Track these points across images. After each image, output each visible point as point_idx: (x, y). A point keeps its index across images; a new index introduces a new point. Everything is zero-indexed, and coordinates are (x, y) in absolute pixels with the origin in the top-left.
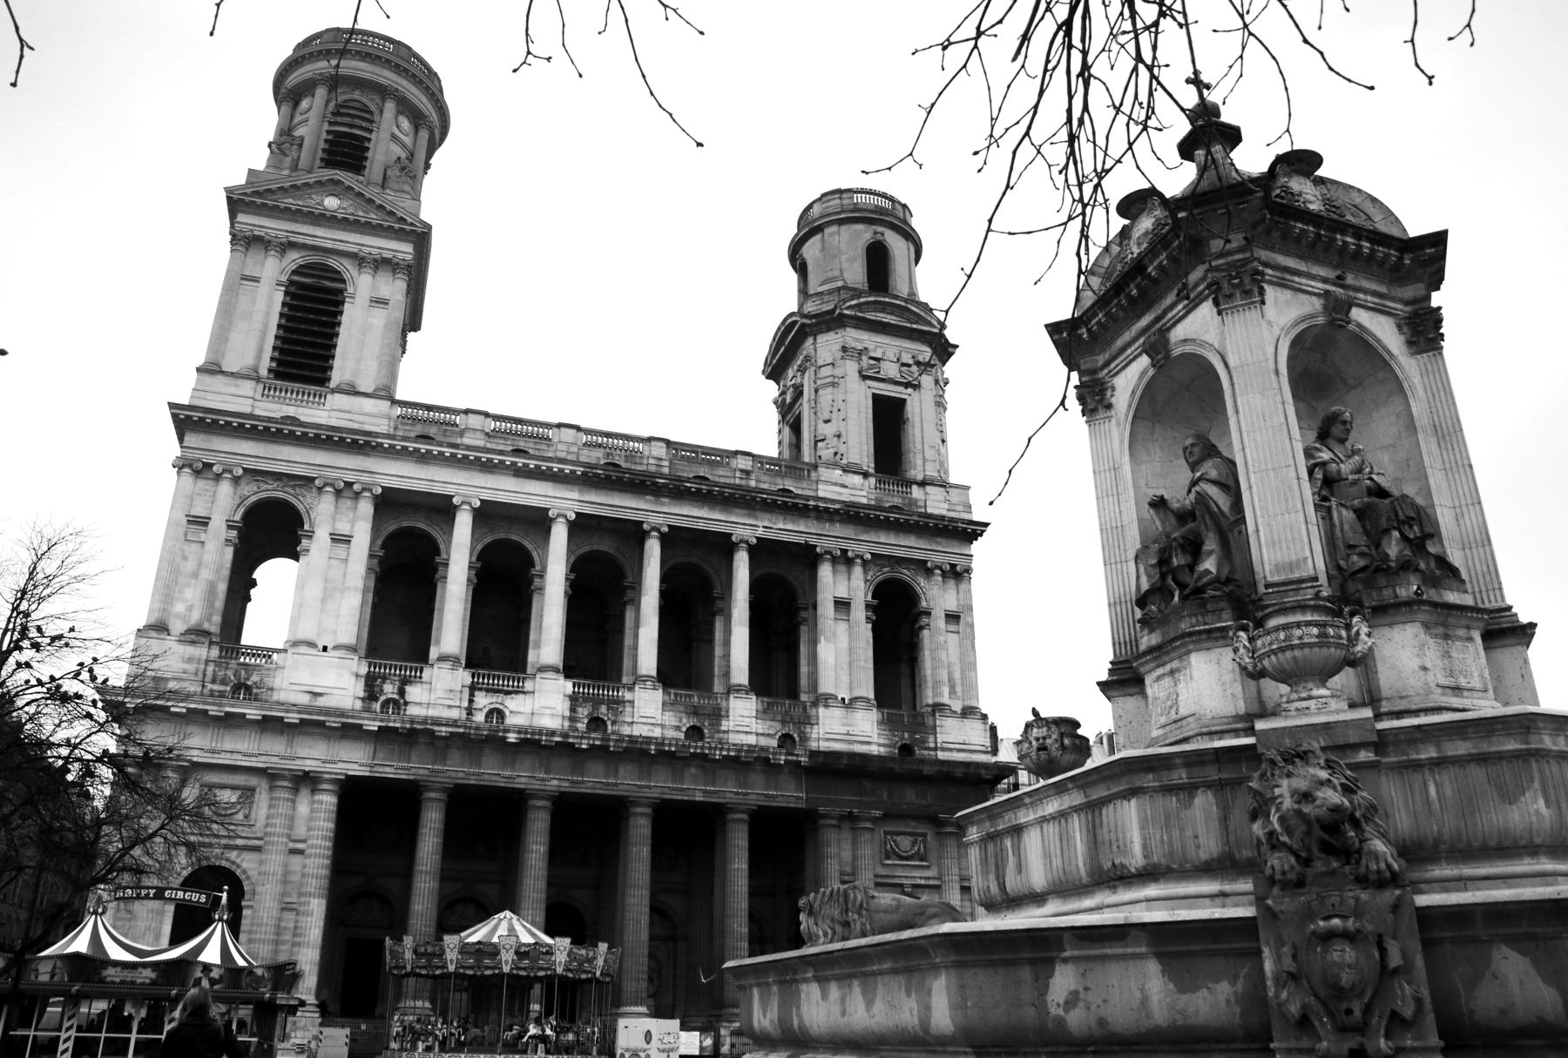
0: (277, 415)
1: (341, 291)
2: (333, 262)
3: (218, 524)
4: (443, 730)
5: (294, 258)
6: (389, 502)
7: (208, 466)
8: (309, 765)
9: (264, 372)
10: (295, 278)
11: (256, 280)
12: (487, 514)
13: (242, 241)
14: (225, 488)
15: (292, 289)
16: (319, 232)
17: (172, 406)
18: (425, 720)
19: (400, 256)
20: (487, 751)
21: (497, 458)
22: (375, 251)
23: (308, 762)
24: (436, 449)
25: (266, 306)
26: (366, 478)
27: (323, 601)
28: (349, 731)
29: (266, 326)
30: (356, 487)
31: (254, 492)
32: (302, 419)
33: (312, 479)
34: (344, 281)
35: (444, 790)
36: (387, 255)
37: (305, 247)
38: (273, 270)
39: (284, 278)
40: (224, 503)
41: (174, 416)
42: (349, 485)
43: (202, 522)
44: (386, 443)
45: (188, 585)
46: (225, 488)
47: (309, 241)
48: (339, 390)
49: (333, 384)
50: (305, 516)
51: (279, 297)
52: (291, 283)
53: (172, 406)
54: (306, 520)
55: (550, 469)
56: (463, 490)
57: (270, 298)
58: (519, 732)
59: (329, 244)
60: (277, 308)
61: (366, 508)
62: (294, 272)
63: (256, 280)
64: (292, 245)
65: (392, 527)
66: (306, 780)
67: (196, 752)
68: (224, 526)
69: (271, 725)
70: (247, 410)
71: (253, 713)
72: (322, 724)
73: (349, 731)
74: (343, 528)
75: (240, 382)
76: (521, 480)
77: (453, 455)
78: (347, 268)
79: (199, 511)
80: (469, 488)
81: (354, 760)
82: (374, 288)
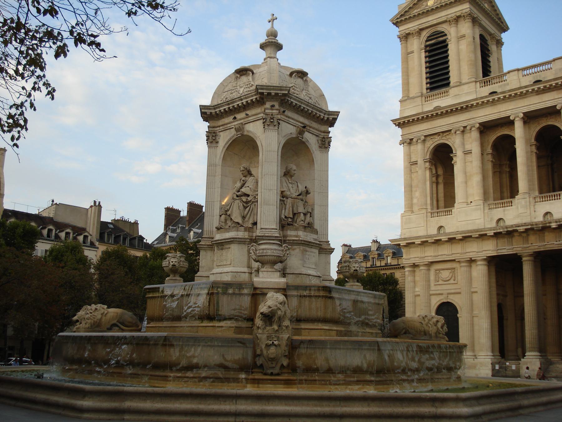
0: (431, 108)
1: (445, 41)
2: (440, 28)
3: (420, 161)
4: (521, 229)
5: (425, 34)
6: (485, 128)
7: (411, 140)
8: (472, 255)
9: (425, 91)
10: (428, 43)
11: (412, 52)
12: (529, 118)
13: (405, 37)
14: (419, 147)
15: (428, 48)
16: (430, 18)
17: (392, 121)
18: (512, 226)
19: (464, 11)
20: (546, 234)
21: (524, 90)
22: (453, 15)
23: (471, 254)
24: (496, 97)
25: (419, 61)
26: (472, 122)
27: (466, 183)
28: (483, 237)
29: (421, 71)
30: (468, 128)
31: (431, 144)
32: (442, 105)
33: (450, 130)
34: (446, 35)
35: (530, 255)
36: (458, 14)
37: (427, 28)
38: (417, 45)
39: (423, 46)
40: (421, 152)
41: (395, 124)
42: (465, 127)
43: (415, 163)
44: (474, 103)
45: (416, 191)
46: (419, 147)
47: (427, 25)
48: (453, 87)
49: (451, 84)
50: (452, 147)
51: (423, 55)
52: (426, 46)
53: (392, 121)
54: (453, 149)
55: (551, 85)
56: (514, 111)
57: (420, 58)
58: (556, 222)
59: (435, 22)
60: (423, 60)
61: (475, 134)
62: (427, 41)
63: (412, 52)
64: (422, 30)
65: (493, 137)
66: (471, 261)
67: (430, 258)
68: (423, 162)
69: (451, 240)
70: (420, 111)
71: (444, 238)
72: (470, 237)
73: (483, 237)
74: (468, 147)
75: (415, 99)
76: (540, 96)
77: (505, 97)
78: (444, 28)
79: (413, 159)
80: (515, 109)
81: (490, 249)
82: (457, 32)
